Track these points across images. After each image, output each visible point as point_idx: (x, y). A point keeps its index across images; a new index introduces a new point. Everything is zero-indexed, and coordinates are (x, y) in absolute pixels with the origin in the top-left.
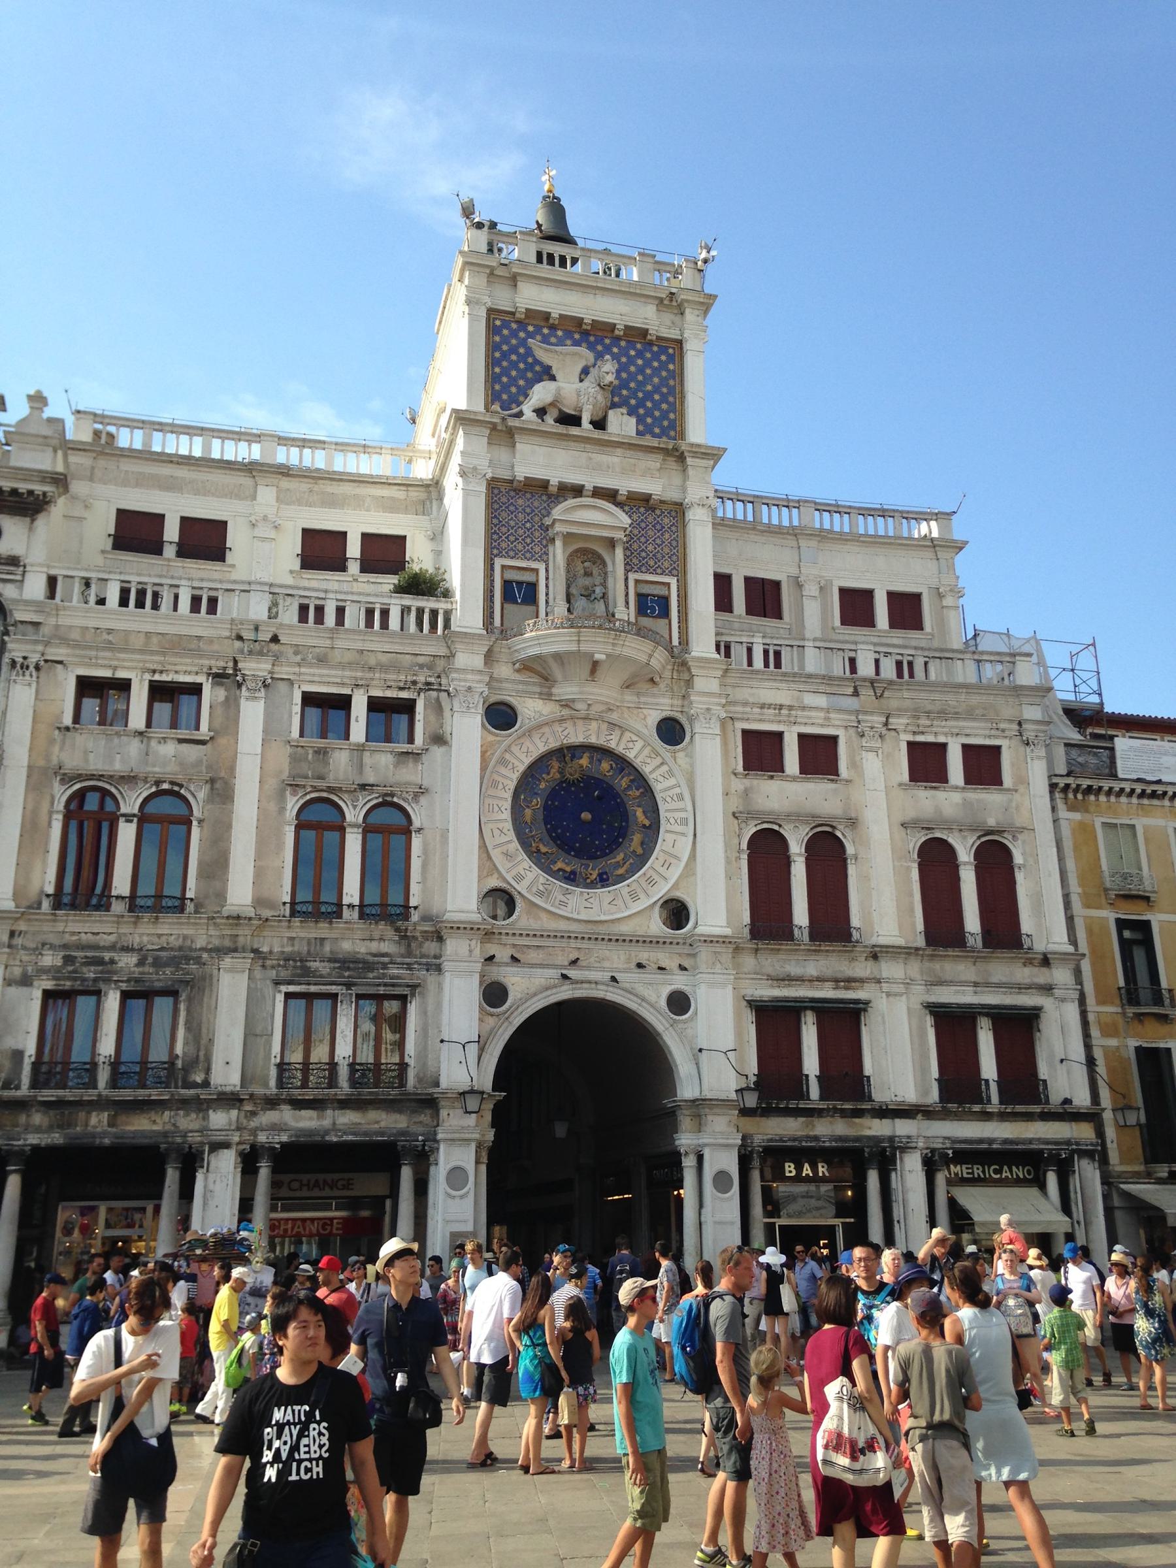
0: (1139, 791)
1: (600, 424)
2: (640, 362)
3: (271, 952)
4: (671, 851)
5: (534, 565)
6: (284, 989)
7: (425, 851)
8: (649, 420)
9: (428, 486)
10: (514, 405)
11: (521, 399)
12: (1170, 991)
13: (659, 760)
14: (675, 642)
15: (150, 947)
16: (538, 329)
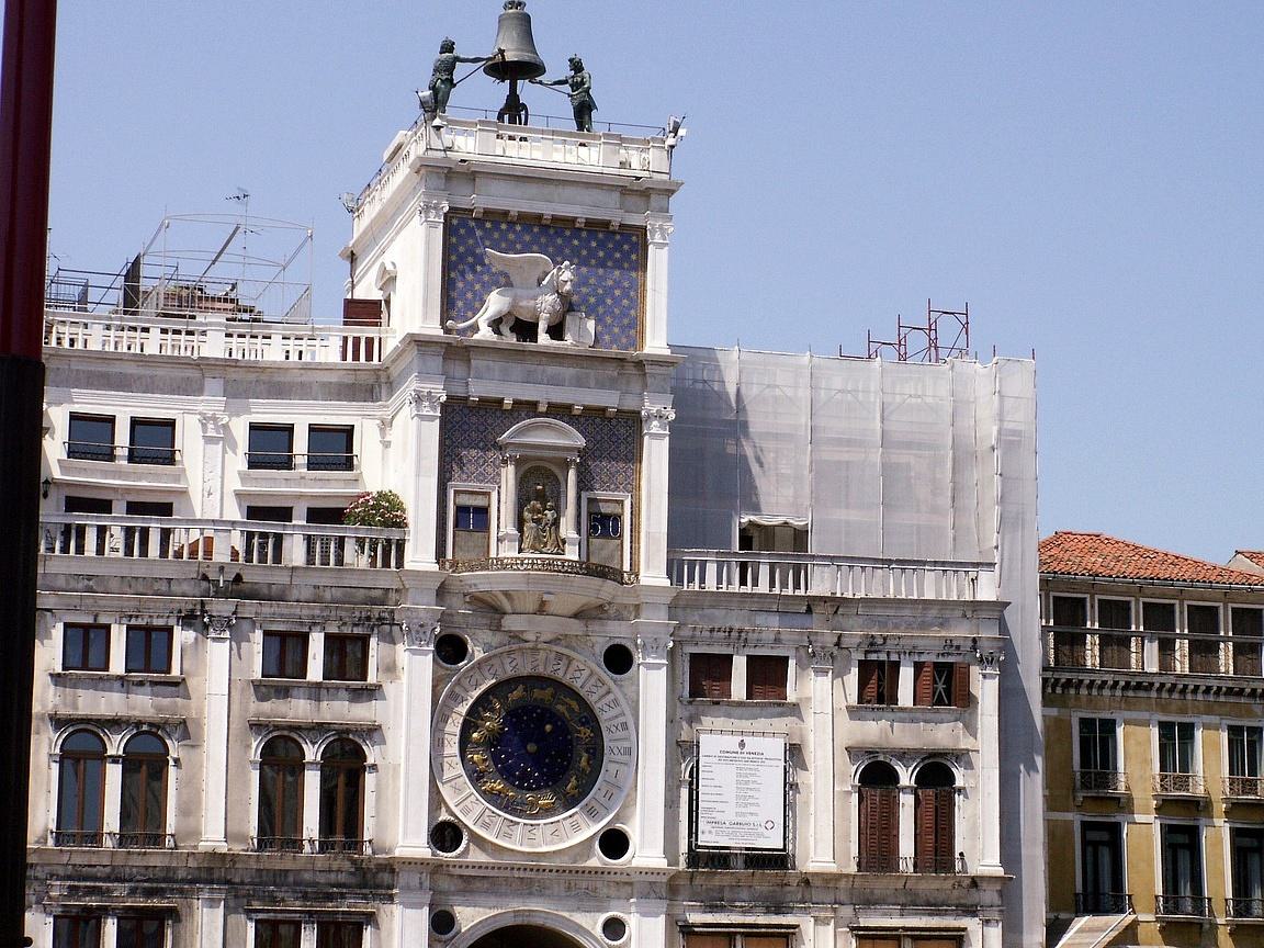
0: (1122, 683)
1: (556, 331)
2: (601, 254)
3: (242, 883)
4: (613, 780)
5: (485, 487)
6: (254, 916)
7: (378, 785)
8: (609, 320)
9: (379, 370)
10: (470, 314)
11: (477, 305)
12: (1130, 896)
13: (605, 688)
14: (626, 567)
15: (139, 877)
16: (496, 225)
